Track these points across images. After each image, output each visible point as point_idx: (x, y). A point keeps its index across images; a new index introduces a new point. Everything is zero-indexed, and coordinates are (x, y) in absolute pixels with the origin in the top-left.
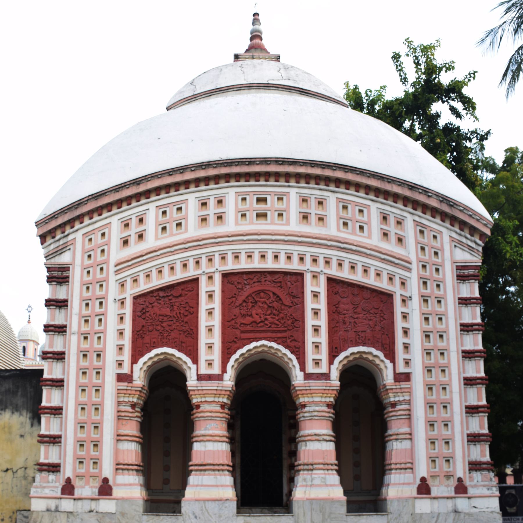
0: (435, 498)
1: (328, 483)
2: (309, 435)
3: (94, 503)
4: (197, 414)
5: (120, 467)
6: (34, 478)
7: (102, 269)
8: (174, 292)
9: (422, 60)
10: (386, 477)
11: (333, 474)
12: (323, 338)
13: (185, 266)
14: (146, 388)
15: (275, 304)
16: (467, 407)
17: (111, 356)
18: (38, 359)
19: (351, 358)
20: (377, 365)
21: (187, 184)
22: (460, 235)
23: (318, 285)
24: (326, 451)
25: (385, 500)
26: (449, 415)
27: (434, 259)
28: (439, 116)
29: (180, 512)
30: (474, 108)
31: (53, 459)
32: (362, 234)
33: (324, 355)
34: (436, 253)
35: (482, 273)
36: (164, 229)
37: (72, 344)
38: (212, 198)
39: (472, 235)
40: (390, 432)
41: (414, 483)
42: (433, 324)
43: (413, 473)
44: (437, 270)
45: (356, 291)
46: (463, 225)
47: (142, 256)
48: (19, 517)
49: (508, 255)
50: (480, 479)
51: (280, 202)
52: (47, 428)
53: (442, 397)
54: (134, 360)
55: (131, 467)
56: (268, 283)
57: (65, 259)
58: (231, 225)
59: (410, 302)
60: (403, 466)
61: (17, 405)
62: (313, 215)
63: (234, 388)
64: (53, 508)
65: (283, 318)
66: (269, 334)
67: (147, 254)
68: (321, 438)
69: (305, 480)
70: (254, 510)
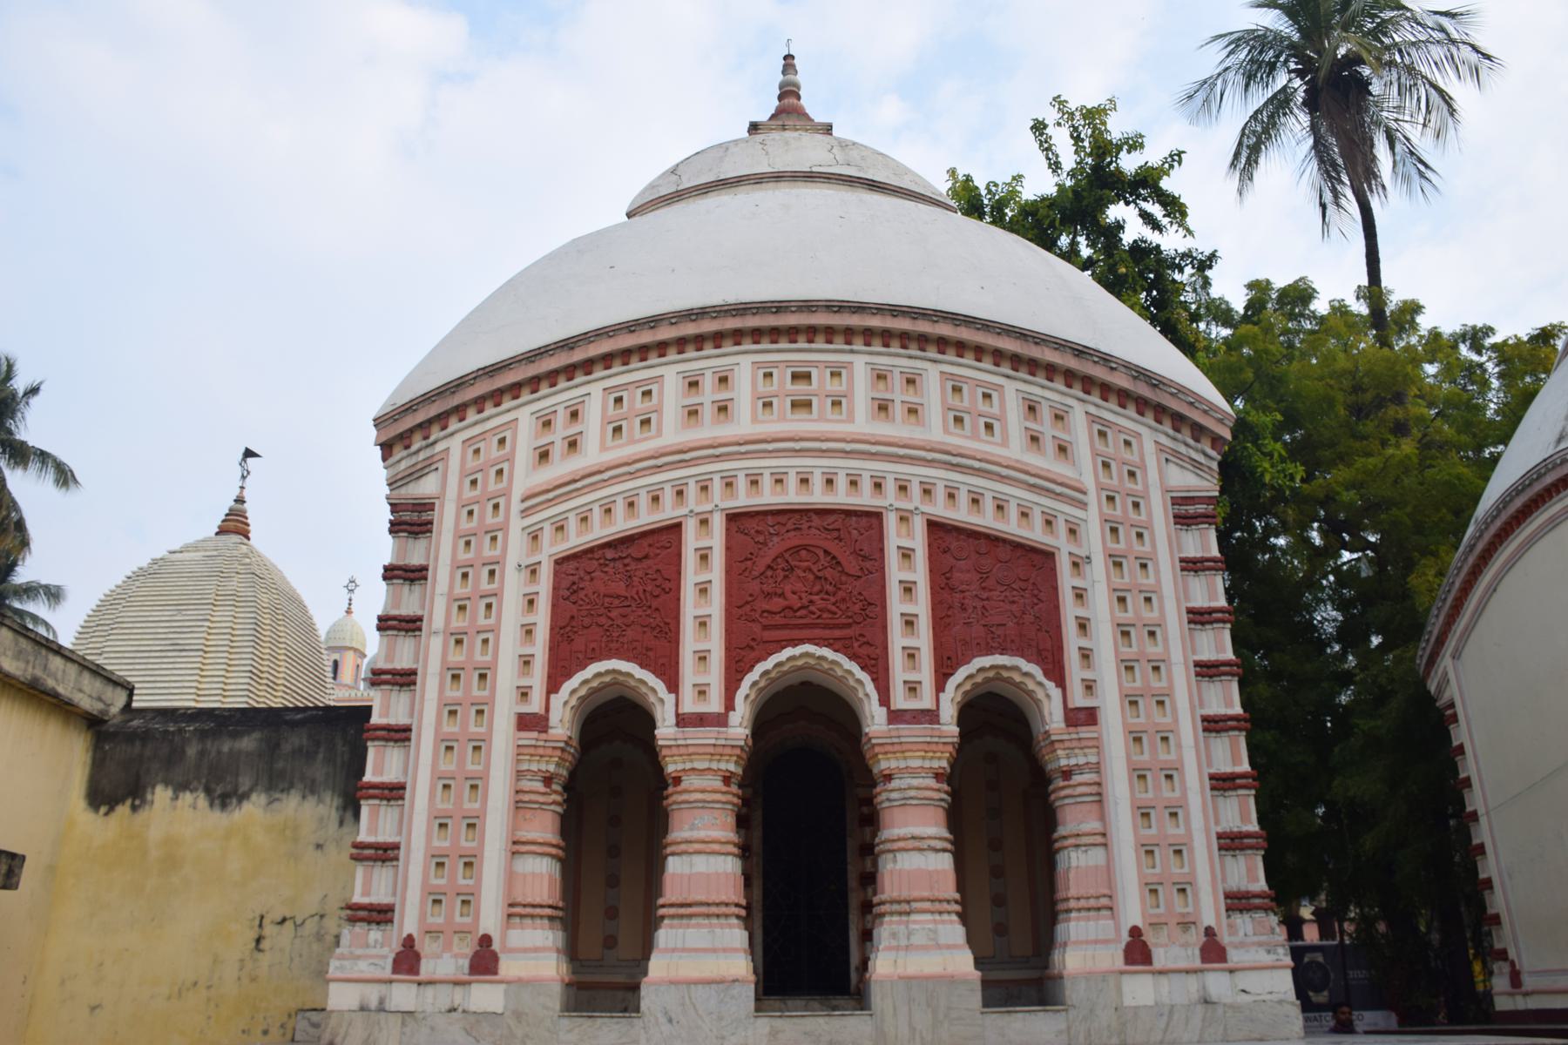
0: (1161, 972)
1: (942, 941)
2: (899, 839)
3: (459, 990)
4: (675, 797)
5: (517, 911)
6: (337, 938)
7: (496, 507)
8: (634, 551)
9: (1086, 132)
10: (1060, 928)
11: (951, 922)
12: (923, 640)
13: (656, 499)
14: (575, 743)
15: (828, 573)
16: (1212, 777)
17: (506, 677)
18: (362, 685)
19: (979, 679)
20: (1030, 693)
21: (662, 347)
22: (1175, 439)
23: (910, 535)
24: (937, 872)
25: (1061, 977)
26: (1177, 794)
27: (1129, 485)
28: (1122, 228)
29: (637, 1010)
30: (1184, 214)
31: (380, 897)
32: (990, 439)
33: (925, 673)
34: (1132, 474)
35: (1221, 512)
36: (617, 430)
37: (431, 655)
38: (708, 374)
39: (1197, 440)
40: (1062, 831)
41: (1117, 940)
42: (1135, 609)
43: (1113, 917)
44: (1136, 505)
45: (983, 546)
46: (1178, 420)
47: (575, 481)
48: (302, 1025)
49: (1267, 478)
50: (1249, 928)
51: (836, 380)
52: (373, 829)
53: (1163, 756)
54: (553, 686)
55: (538, 911)
56: (814, 531)
57: (426, 487)
58: (744, 424)
59: (1087, 567)
60: (1092, 903)
61: (313, 781)
62: (898, 405)
63: (750, 742)
64: (374, 1004)
65: (844, 600)
66: (818, 632)
67: (584, 477)
68: (924, 844)
69: (894, 935)
70: (790, 1003)
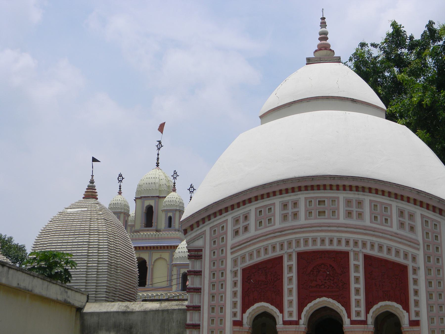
12: (362, 297)
33: (362, 309)
54: (244, 311)
57: (198, 244)
